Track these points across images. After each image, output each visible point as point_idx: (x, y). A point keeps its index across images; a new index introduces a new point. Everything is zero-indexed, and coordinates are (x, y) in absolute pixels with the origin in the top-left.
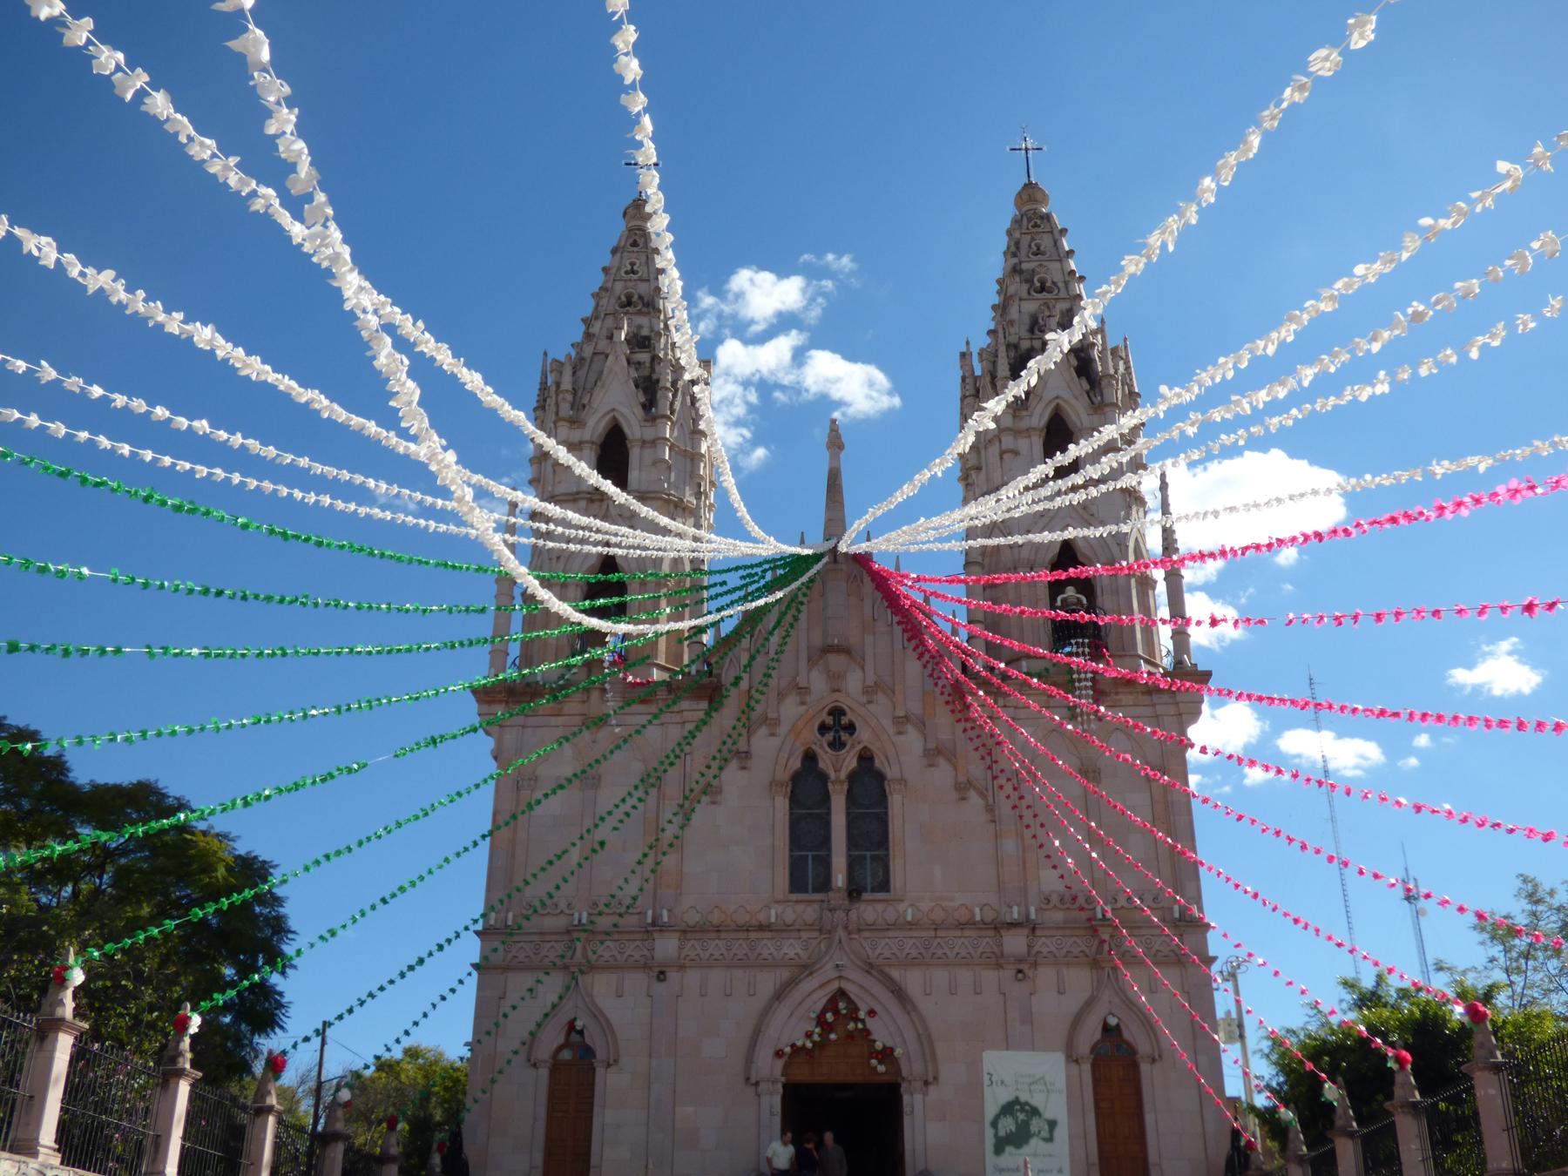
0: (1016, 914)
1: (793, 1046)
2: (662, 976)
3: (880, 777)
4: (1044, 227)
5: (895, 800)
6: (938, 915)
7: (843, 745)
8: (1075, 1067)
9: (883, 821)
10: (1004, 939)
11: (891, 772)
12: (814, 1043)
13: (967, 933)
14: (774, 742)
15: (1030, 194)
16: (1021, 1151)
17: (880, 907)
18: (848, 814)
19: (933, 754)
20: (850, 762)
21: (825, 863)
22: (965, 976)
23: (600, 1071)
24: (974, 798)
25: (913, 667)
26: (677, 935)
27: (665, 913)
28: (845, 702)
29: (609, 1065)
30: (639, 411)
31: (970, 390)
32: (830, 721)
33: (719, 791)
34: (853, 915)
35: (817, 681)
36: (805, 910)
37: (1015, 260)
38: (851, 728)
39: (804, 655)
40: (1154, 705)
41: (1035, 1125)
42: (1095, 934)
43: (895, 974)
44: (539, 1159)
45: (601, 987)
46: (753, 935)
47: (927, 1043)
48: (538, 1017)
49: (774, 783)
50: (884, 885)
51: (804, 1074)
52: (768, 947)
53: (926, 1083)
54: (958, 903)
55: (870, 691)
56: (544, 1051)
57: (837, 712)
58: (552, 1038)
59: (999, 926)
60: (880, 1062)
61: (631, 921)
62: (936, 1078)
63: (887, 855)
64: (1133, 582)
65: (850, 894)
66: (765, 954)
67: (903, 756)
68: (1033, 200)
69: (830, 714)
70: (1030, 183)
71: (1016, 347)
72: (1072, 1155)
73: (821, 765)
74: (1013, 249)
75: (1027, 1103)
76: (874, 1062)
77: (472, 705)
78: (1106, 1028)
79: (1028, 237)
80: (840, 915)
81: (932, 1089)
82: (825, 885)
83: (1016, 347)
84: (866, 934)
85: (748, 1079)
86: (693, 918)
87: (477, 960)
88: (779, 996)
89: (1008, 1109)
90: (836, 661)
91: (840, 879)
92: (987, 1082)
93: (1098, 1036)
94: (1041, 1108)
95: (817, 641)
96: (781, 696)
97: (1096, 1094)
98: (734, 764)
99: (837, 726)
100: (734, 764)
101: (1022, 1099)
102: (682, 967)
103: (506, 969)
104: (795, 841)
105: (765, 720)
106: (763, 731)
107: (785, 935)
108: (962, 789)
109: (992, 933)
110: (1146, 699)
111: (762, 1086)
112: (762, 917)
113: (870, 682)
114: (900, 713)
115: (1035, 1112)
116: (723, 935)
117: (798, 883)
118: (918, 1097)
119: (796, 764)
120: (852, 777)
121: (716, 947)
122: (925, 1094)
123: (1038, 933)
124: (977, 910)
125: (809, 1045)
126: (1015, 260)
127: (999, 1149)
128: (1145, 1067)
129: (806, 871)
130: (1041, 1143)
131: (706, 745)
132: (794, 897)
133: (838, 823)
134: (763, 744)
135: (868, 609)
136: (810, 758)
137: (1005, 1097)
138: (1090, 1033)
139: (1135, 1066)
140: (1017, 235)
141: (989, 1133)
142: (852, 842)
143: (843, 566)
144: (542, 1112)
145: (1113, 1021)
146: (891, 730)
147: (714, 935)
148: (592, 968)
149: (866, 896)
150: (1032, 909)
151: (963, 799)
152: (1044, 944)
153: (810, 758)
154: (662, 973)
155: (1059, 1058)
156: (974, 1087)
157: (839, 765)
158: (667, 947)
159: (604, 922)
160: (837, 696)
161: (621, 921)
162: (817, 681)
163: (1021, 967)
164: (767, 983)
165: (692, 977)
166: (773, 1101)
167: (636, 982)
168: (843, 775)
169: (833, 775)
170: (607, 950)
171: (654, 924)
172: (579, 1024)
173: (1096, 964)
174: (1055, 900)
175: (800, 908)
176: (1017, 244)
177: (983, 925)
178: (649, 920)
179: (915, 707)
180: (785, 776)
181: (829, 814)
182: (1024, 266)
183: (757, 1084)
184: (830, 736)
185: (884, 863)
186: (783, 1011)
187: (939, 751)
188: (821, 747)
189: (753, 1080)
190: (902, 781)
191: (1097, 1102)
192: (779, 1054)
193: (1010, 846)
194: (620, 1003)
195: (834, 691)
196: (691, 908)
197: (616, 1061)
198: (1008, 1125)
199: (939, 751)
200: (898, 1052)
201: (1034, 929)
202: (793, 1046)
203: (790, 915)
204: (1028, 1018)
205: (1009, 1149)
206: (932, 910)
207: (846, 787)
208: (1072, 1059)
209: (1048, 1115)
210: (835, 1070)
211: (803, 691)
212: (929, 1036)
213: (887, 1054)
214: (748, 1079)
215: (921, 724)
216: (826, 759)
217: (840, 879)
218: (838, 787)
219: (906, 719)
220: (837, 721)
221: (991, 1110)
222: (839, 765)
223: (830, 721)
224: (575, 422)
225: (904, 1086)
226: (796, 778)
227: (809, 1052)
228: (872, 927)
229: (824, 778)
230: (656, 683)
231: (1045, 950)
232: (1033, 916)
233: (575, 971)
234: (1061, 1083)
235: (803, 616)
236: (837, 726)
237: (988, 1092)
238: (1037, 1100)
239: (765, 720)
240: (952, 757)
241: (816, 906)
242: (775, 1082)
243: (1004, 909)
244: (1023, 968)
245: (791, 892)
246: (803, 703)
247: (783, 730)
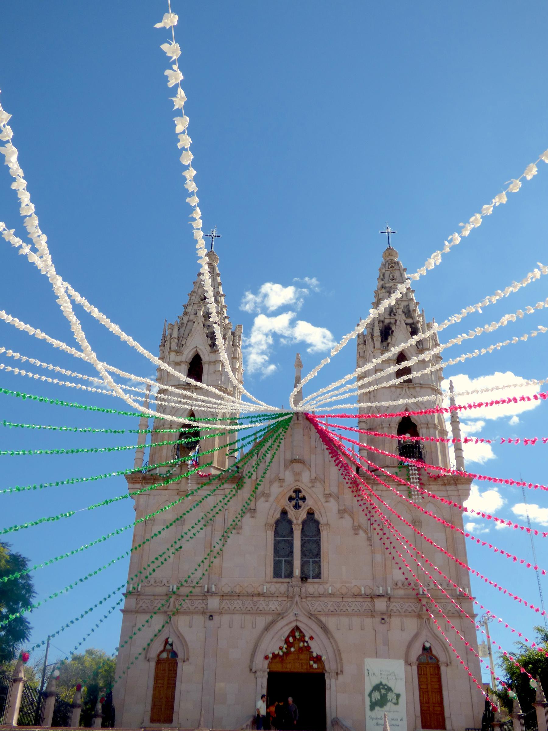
0: (381, 591)
1: (273, 654)
2: (211, 617)
3: (317, 523)
4: (396, 267)
5: (324, 535)
6: (344, 591)
7: (300, 507)
8: (409, 667)
9: (318, 544)
10: (374, 602)
11: (322, 521)
12: (284, 653)
13: (357, 599)
14: (267, 505)
15: (390, 252)
16: (383, 709)
17: (316, 586)
18: (302, 540)
19: (343, 512)
20: (303, 515)
21: (290, 563)
22: (356, 621)
23: (180, 664)
24: (361, 532)
25: (334, 471)
26: (219, 597)
27: (213, 586)
28: (301, 487)
29: (184, 661)
30: (208, 348)
31: (362, 341)
32: (294, 495)
33: (241, 528)
34: (303, 590)
35: (288, 476)
36: (281, 586)
37: (383, 282)
38: (304, 499)
39: (282, 464)
40: (447, 491)
41: (390, 696)
42: (420, 603)
43: (323, 619)
44: (149, 707)
45: (182, 622)
46: (255, 598)
47: (338, 653)
48: (152, 636)
49: (267, 524)
50: (318, 576)
51: (278, 667)
52: (262, 604)
53: (337, 674)
54: (353, 585)
55: (313, 481)
56: (154, 653)
57: (297, 491)
58: (158, 646)
59: (373, 597)
60: (315, 663)
61: (197, 590)
62: (342, 671)
63: (320, 561)
64: (437, 432)
65: (302, 579)
66: (261, 608)
67: (327, 513)
68: (390, 255)
69: (294, 492)
70: (390, 248)
71: (383, 322)
72: (407, 711)
73: (289, 516)
74: (382, 277)
75: (386, 685)
76: (312, 662)
77: (125, 484)
78: (424, 648)
79: (389, 272)
80: (297, 589)
81: (340, 677)
82: (290, 575)
83: (383, 322)
84: (309, 599)
85: (251, 670)
86: (226, 590)
87: (123, 608)
88: (267, 629)
89: (377, 688)
90: (297, 467)
91: (297, 572)
92: (366, 674)
93: (420, 652)
94: (393, 689)
95: (289, 457)
96: (271, 482)
97: (419, 681)
98: (248, 515)
99: (297, 497)
100: (248, 515)
101: (384, 683)
102: (221, 613)
103: (137, 612)
104: (276, 552)
105: (263, 494)
106: (262, 499)
107: (271, 598)
108: (356, 529)
109: (369, 600)
110: (443, 488)
111: (258, 673)
112: (260, 590)
113: (313, 477)
114: (327, 492)
115: (390, 689)
116: (241, 598)
117: (277, 574)
118: (333, 681)
119: (278, 515)
120: (304, 523)
121: (237, 604)
122: (337, 679)
123: (392, 600)
124: (363, 589)
125: (281, 653)
126: (383, 282)
127: (372, 708)
128: (443, 668)
130: (393, 705)
131: (235, 505)
132: (275, 580)
133: (297, 544)
134: (262, 506)
135: (313, 443)
136: (284, 513)
137: (375, 681)
138: (417, 651)
139: (438, 668)
140: (383, 271)
141: (367, 699)
142: (303, 554)
143: (301, 422)
144: (151, 684)
145: (427, 645)
146: (323, 500)
147: (236, 598)
148: (177, 613)
149: (310, 580)
150: (389, 589)
151: (357, 534)
152: (395, 606)
153: (284, 513)
154: (211, 616)
155: (402, 662)
156: (360, 676)
157: (298, 517)
158: (214, 603)
159: (184, 590)
160: (298, 483)
161: (194, 590)
163: (384, 617)
164: (262, 622)
165: (226, 618)
166: (263, 681)
167: (199, 620)
168: (300, 521)
169: (295, 521)
170: (186, 604)
171: (208, 592)
172: (170, 641)
173: (419, 616)
174: (400, 584)
175: (278, 585)
176: (384, 275)
177: (366, 596)
178: (206, 590)
179: (334, 489)
180: (272, 521)
181: (292, 540)
182: (387, 285)
183: (255, 672)
184: (294, 502)
185: (318, 564)
186: (269, 636)
187: (345, 511)
188: (290, 507)
189: (254, 670)
190: (328, 524)
191: (420, 685)
192: (266, 658)
193: (378, 557)
194: (190, 631)
195: (296, 481)
196: (226, 584)
197: (188, 659)
198: (376, 696)
199: (345, 511)
200: (324, 658)
201: (390, 598)
202: (273, 654)
203: (273, 588)
204: (386, 642)
205: (377, 708)
206: (341, 588)
207: (301, 527)
208: (408, 663)
209: (396, 691)
210: (293, 666)
211: (282, 480)
212: (339, 650)
213: (318, 659)
214: (251, 670)
215: (337, 498)
216: (292, 514)
217: (297, 572)
218: (297, 527)
219: (330, 495)
220: (298, 496)
221: (368, 688)
222: (298, 517)
223: (294, 495)
224: (178, 352)
225: (326, 675)
226: (277, 523)
227: (281, 657)
228: (312, 596)
229: (290, 522)
230: (213, 476)
231: (395, 609)
232: (389, 592)
233: (170, 615)
234: (403, 676)
235: (282, 445)
236: (297, 497)
237: (367, 679)
238: (391, 684)
239: (263, 494)
240: (351, 514)
241: (286, 585)
242: (264, 671)
243: (375, 588)
244: (384, 618)
245: (274, 578)
246: (281, 486)
247: (272, 499)
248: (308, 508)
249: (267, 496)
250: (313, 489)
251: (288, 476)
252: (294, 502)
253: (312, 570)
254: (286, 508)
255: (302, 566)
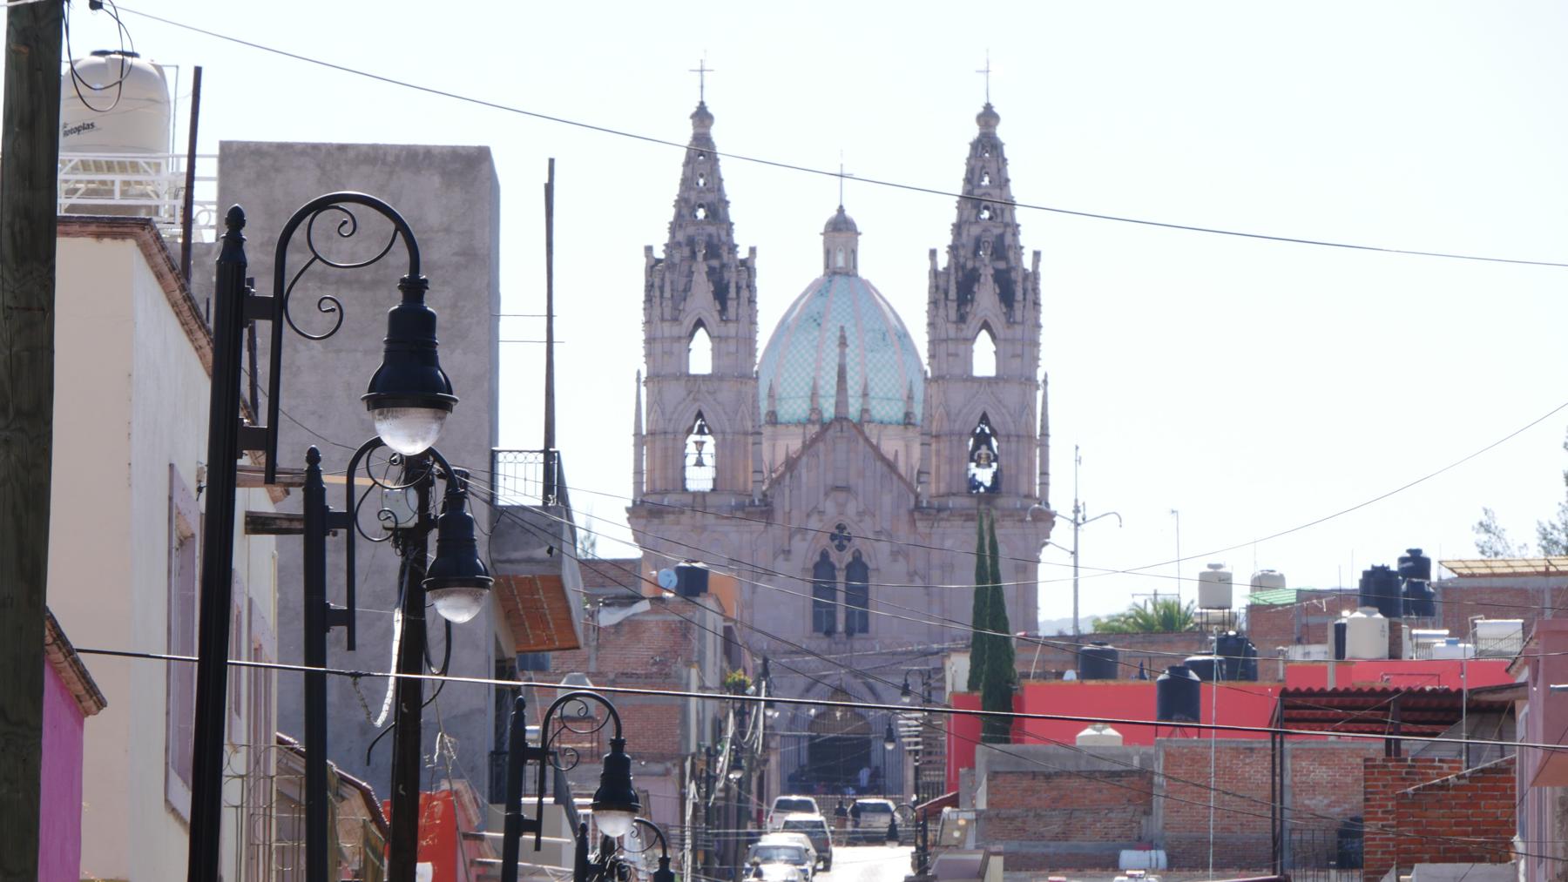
3: (865, 567)
11: (871, 565)
19: (895, 554)
20: (848, 557)
36: (822, 643)
55: (860, 514)
57: (841, 528)
67: (878, 555)
90: (841, 496)
91: (840, 627)
98: (782, 557)
99: (840, 536)
106: (798, 537)
117: (817, 627)
119: (817, 558)
120: (849, 567)
129: (823, 622)
153: (824, 555)
157: (841, 560)
162: (830, 507)
180: (810, 565)
190: (877, 570)
203: (813, 646)
211: (822, 513)
215: (890, 536)
216: (834, 556)
217: (840, 627)
222: (841, 560)
226: (816, 566)
229: (833, 567)
236: (840, 536)
249: (803, 530)
251: (830, 507)
253: (859, 625)
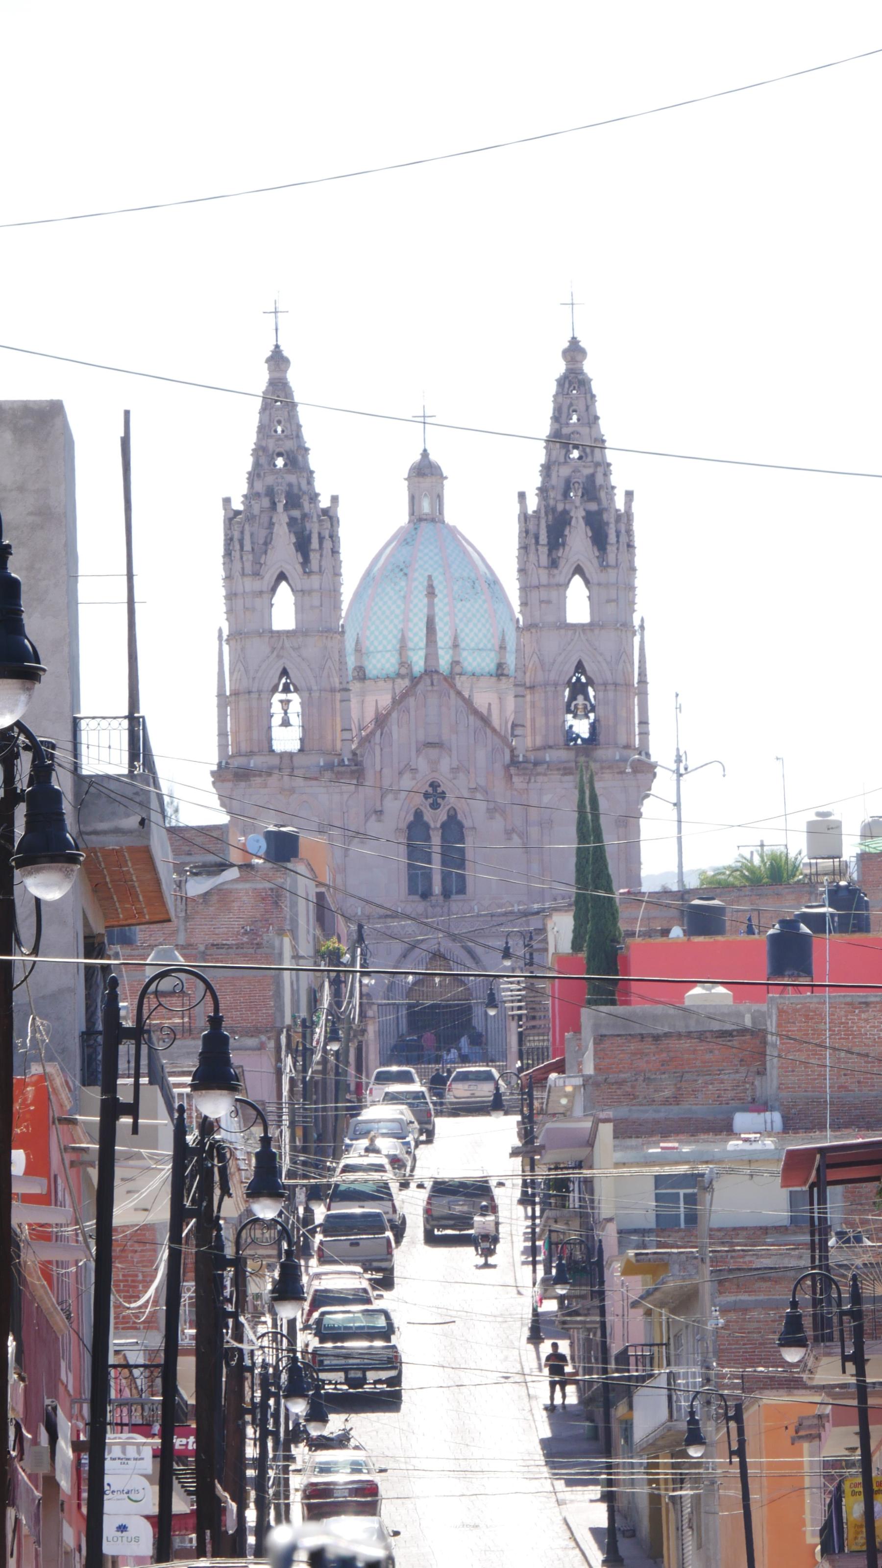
3: (461, 826)
11: (467, 823)
32: (430, 790)
55: (455, 770)
57: (434, 785)
90: (433, 753)
91: (437, 889)
99: (435, 794)
113: (455, 764)
119: (411, 818)
120: (444, 826)
136: (418, 814)
149: (454, 897)
153: (418, 814)
157: (435, 819)
168: (438, 825)
180: (404, 826)
211: (414, 770)
217: (437, 889)
218: (436, 832)
222: (435, 819)
229: (427, 826)
236: (435, 794)
246: (414, 779)
248: (449, 806)
250: (454, 781)
251: (422, 764)
252: (431, 800)
253: (455, 886)
254: (421, 808)
255: (443, 880)
